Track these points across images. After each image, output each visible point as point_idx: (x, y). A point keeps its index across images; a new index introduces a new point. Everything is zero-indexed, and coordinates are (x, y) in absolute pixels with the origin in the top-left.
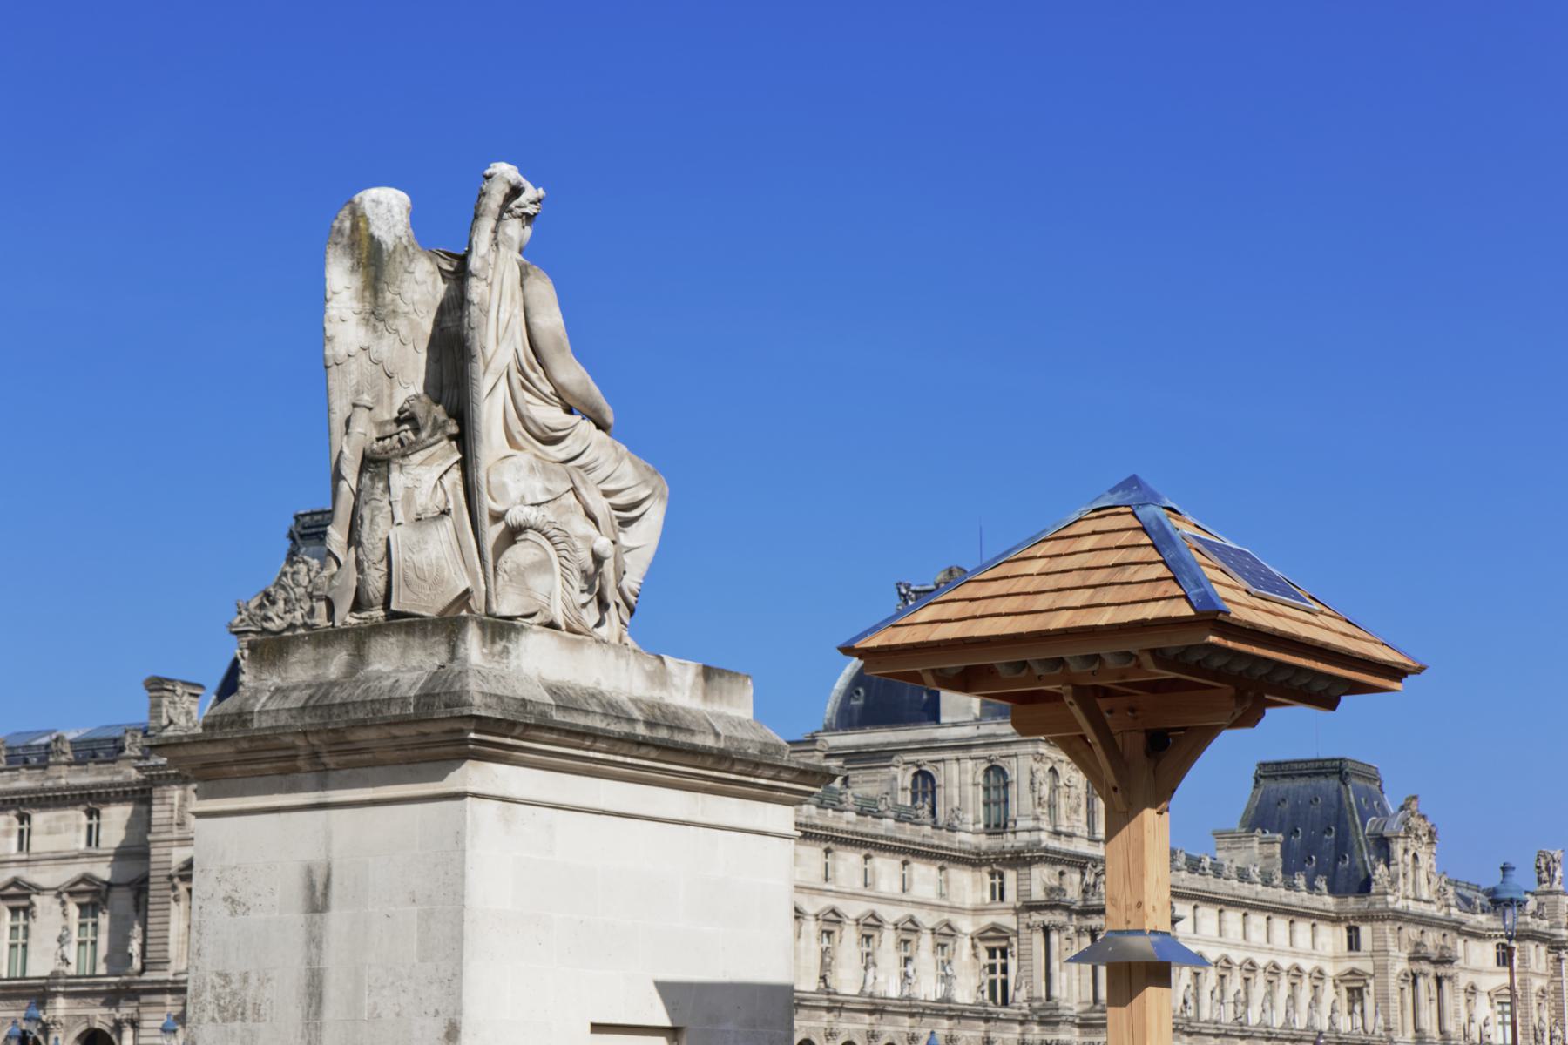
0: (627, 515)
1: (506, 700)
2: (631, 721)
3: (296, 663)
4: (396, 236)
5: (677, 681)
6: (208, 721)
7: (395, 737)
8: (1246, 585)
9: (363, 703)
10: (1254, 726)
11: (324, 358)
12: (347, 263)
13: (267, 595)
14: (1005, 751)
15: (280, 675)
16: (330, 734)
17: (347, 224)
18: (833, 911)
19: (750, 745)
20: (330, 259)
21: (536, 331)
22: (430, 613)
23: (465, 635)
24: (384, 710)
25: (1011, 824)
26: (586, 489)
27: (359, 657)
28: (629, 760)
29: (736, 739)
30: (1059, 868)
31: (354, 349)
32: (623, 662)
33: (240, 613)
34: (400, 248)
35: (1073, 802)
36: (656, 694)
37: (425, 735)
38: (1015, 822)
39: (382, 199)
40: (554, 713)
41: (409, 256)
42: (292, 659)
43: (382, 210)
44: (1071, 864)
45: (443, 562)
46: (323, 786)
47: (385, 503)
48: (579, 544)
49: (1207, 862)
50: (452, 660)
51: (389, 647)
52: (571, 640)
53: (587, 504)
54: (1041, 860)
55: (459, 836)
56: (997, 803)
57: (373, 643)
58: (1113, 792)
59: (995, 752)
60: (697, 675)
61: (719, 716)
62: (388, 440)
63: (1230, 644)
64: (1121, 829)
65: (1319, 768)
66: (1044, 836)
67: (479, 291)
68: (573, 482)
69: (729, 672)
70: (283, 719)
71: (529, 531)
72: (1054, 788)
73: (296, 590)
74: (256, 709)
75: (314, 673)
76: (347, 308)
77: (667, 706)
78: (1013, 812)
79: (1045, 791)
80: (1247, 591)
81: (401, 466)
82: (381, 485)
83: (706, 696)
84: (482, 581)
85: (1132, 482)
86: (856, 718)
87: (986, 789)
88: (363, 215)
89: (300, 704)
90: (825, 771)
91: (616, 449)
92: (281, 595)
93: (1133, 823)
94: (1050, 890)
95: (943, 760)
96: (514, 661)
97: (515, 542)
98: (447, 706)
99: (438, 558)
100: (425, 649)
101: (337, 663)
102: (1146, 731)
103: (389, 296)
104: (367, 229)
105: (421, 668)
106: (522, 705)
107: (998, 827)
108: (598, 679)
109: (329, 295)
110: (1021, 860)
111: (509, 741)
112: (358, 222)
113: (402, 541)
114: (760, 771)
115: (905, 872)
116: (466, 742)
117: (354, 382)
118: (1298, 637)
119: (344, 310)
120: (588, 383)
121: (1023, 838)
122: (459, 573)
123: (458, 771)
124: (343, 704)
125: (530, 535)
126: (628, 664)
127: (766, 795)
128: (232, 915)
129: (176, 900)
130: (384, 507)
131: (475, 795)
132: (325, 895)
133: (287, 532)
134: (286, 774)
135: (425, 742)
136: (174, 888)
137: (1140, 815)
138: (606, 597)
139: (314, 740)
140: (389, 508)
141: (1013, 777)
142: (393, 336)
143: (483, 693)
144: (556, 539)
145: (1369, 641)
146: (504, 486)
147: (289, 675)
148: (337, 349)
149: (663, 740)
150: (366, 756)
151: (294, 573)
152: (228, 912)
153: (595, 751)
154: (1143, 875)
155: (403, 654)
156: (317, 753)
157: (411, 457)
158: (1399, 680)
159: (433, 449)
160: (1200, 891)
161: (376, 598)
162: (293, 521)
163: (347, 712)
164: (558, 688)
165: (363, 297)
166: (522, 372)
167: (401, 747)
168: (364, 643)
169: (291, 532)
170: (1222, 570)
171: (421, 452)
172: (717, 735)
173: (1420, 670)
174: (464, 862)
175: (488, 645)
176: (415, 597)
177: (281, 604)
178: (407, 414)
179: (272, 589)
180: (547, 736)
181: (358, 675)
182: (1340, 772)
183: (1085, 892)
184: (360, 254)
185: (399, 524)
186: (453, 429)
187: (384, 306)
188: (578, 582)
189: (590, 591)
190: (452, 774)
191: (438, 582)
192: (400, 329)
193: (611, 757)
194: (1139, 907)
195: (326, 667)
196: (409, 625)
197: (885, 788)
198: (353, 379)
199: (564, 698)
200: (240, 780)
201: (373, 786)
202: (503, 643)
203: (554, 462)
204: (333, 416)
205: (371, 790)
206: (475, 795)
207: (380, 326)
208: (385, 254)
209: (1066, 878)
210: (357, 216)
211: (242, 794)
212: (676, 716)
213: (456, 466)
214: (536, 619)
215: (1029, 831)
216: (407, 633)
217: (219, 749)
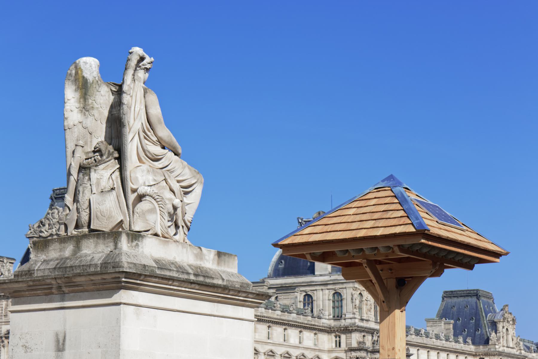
0: (187, 190)
1: (137, 265)
2: (188, 274)
3: (52, 250)
4: (93, 77)
5: (207, 257)
6: (16, 274)
7: (92, 280)
8: (436, 219)
9: (79, 266)
10: (440, 276)
11: (64, 126)
12: (74, 87)
13: (41, 222)
14: (341, 286)
15: (45, 255)
16: (66, 279)
17: (74, 72)
18: (271, 351)
20: (67, 86)
21: (150, 115)
22: (107, 230)
23: (121, 239)
24: (88, 269)
25: (343, 316)
26: (170, 179)
27: (78, 248)
28: (187, 290)
29: (231, 281)
30: (363, 334)
31: (76, 122)
32: (185, 250)
33: (30, 230)
34: (95, 81)
35: (369, 307)
36: (198, 263)
37: (105, 279)
38: (345, 315)
39: (87, 62)
40: (157, 270)
41: (98, 85)
42: (51, 248)
43: (88, 66)
44: (367, 332)
45: (112, 209)
46: (63, 300)
47: (89, 185)
48: (167, 202)
49: (423, 332)
50: (115, 249)
51: (90, 243)
52: (164, 241)
53: (171, 185)
54: (356, 330)
55: (118, 320)
56: (338, 307)
57: (83, 242)
58: (383, 303)
59: (337, 287)
60: (215, 255)
61: (224, 272)
62: (90, 159)
63: (430, 243)
64: (386, 318)
65: (468, 293)
66: (357, 321)
67: (127, 99)
68: (165, 177)
69: (228, 254)
70: (47, 273)
71: (147, 196)
72: (361, 301)
73: (53, 220)
74: (36, 269)
75: (59, 254)
76: (73, 106)
77: (203, 267)
78: (344, 311)
79: (357, 302)
80: (437, 222)
81: (95, 170)
82: (87, 178)
83: (218, 264)
84: (128, 217)
85: (391, 178)
86: (281, 273)
87: (334, 302)
88: (80, 68)
89: (53, 267)
90: (267, 294)
91: (182, 163)
92: (47, 222)
93: (391, 316)
94: (359, 343)
95: (316, 290)
96: (140, 250)
97: (141, 201)
98: (113, 267)
99: (110, 207)
100: (105, 244)
101: (68, 250)
102: (396, 278)
103: (90, 101)
104: (82, 74)
105: (103, 252)
106: (144, 267)
107: (338, 317)
108: (175, 257)
109: (66, 101)
110: (347, 330)
111: (138, 282)
112: (78, 71)
113: (95, 201)
114: (240, 294)
115: (300, 335)
116: (121, 282)
117: (76, 136)
118: (458, 240)
119: (72, 107)
120: (171, 137)
121: (348, 322)
122: (118, 213)
123: (118, 294)
124: (71, 267)
125: (148, 198)
127: (243, 304)
128: (25, 352)
129: (4, 346)
130: (88, 187)
131: (125, 304)
132: (64, 344)
133: (50, 196)
134: (48, 295)
135: (104, 282)
136: (3, 342)
137: (393, 313)
138: (178, 223)
139: (59, 281)
140: (90, 187)
141: (344, 297)
142: (92, 117)
143: (128, 262)
144: (158, 200)
145: (486, 242)
146: (137, 178)
147: (49, 255)
148: (69, 123)
149: (200, 281)
150: (80, 288)
151: (52, 213)
152: (24, 351)
153: (173, 286)
154: (395, 337)
155: (96, 246)
156: (60, 286)
157: (99, 166)
158: (498, 258)
159: (108, 163)
160: (420, 343)
161: (84, 224)
162: (52, 192)
163: (73, 270)
164: (158, 260)
165: (80, 101)
166: (144, 132)
167: (94, 284)
168: (80, 242)
169: (51, 196)
170: (427, 213)
171: (103, 164)
172: (223, 279)
173: (507, 254)
174: (120, 331)
175: (130, 243)
176: (101, 223)
177: (47, 226)
178: (98, 149)
179: (43, 220)
180: (154, 280)
181: (77, 255)
182: (477, 295)
183: (373, 343)
184: (79, 84)
185: (94, 194)
186: (116, 155)
187: (89, 105)
188: (167, 218)
189: (171, 221)
190: (115, 295)
191: (110, 217)
192: (95, 114)
193: (180, 288)
194: (393, 350)
195: (64, 251)
196: (99, 234)
197: (293, 301)
198: (76, 135)
199: (161, 264)
200: (30, 297)
201: (83, 300)
202: (136, 242)
203: (157, 169)
204: (67, 150)
205: (82, 301)
206: (125, 304)
207: (87, 113)
208: (89, 84)
209: (366, 338)
210: (77, 68)
211: (30, 303)
212: (206, 272)
213: (117, 170)
214: (150, 232)
215: (351, 319)
216: (97, 238)
217: (20, 285)
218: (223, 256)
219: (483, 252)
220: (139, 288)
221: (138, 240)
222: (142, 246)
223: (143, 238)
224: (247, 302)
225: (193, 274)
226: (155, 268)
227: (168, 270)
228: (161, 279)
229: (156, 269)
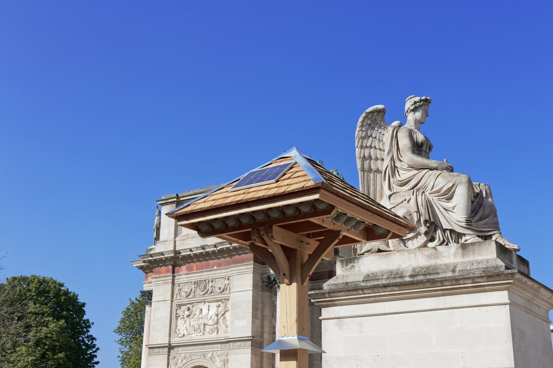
0: (449, 195)
5: (445, 254)
19: (476, 271)
28: (387, 293)
36: (433, 262)
40: (361, 284)
52: (384, 255)
83: (463, 256)
96: (357, 269)
120: (413, 159)
126: (415, 255)
175: (345, 267)
180: (340, 294)
202: (352, 264)
218: (470, 246)
220: (337, 304)
221: (354, 262)
222: (358, 266)
223: (358, 259)
224: (485, 287)
225: (408, 276)
226: (359, 282)
227: (375, 280)
228: (347, 292)
229: (360, 283)
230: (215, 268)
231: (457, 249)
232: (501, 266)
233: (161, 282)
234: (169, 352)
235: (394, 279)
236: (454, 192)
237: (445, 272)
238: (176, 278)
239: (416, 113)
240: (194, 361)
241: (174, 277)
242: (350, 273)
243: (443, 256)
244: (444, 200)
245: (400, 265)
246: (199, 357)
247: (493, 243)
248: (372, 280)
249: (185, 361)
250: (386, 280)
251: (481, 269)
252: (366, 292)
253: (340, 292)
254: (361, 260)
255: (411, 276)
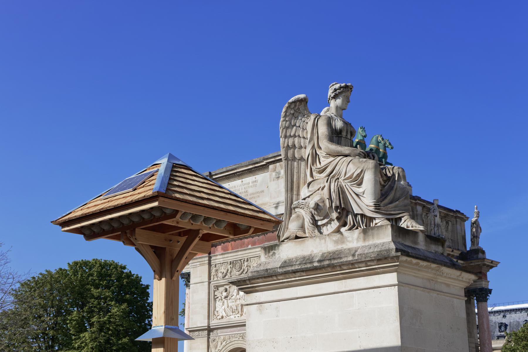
0: (358, 180)
19: (372, 254)
28: (297, 278)
32: (323, 241)
36: (339, 247)
40: (279, 270)
52: (300, 241)
83: (364, 240)
96: (277, 256)
106: (266, 271)
126: (325, 241)
202: (273, 251)
218: (370, 230)
219: (132, 206)
221: (275, 249)
224: (377, 270)
225: (316, 262)
228: (263, 278)
229: (278, 269)
230: (250, 247)
231: (360, 233)
232: (392, 249)
233: (198, 263)
234: (209, 335)
235: (305, 264)
236: (363, 178)
237: (347, 256)
238: (213, 258)
239: (337, 100)
240: (233, 343)
241: (210, 258)
242: (271, 260)
243: (348, 241)
244: (355, 186)
245: (312, 251)
246: (237, 339)
247: (389, 227)
248: (288, 266)
249: (224, 343)
250: (299, 265)
251: (376, 253)
252: (279, 278)
253: (258, 278)
254: (281, 247)
255: (319, 261)
